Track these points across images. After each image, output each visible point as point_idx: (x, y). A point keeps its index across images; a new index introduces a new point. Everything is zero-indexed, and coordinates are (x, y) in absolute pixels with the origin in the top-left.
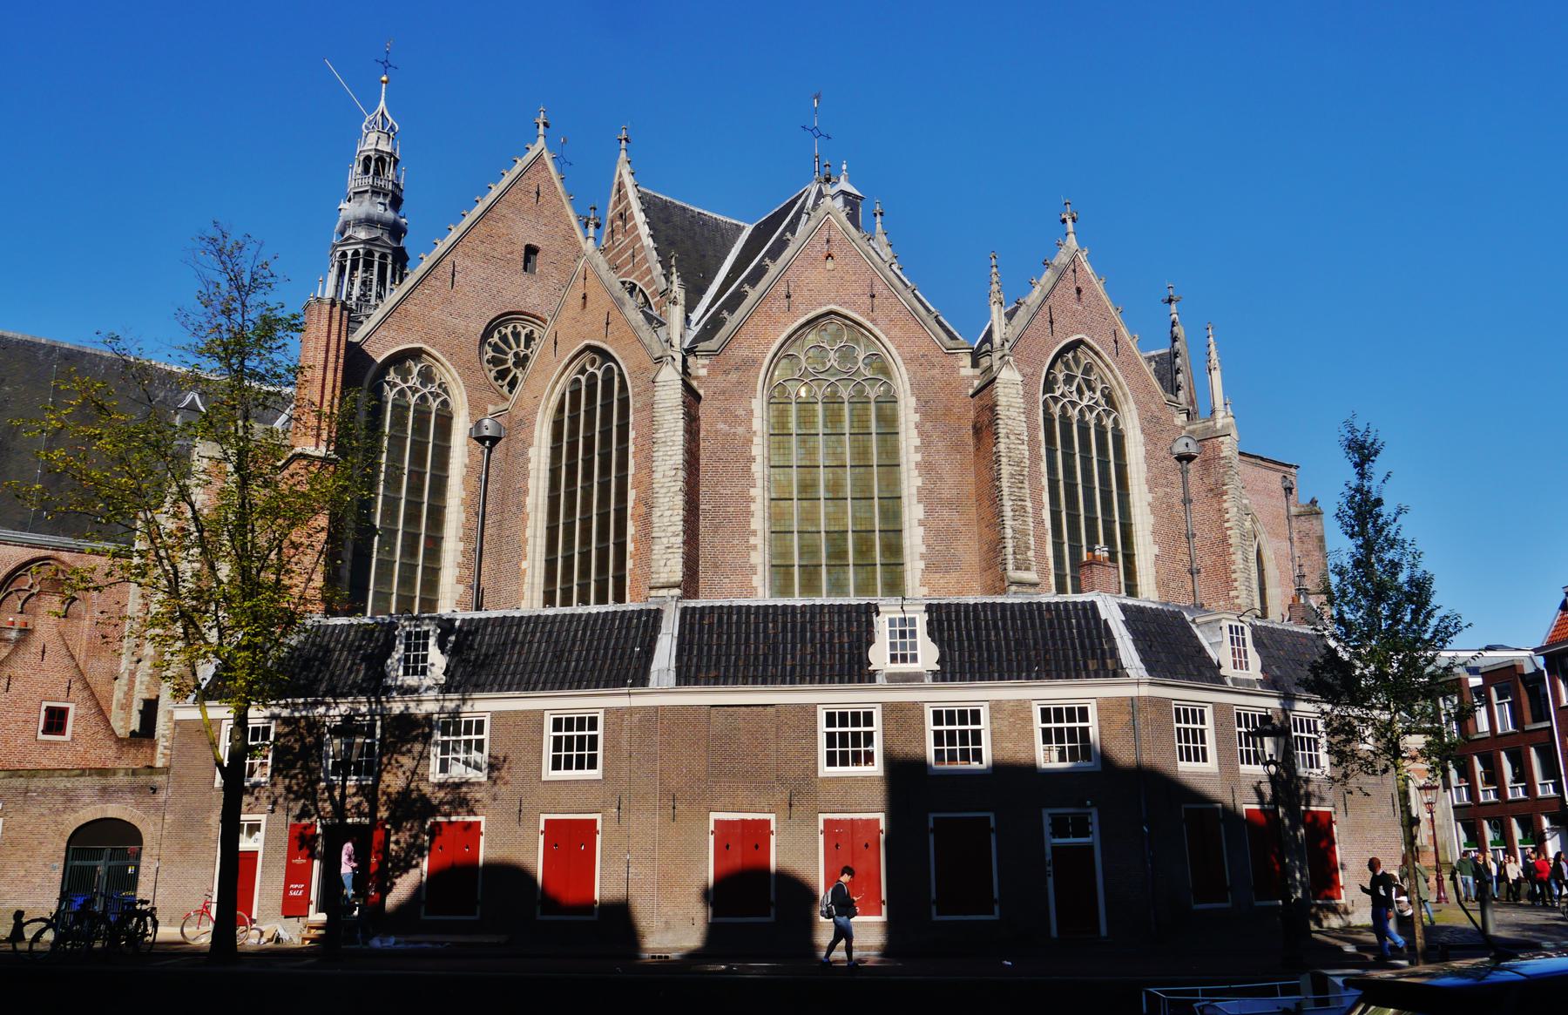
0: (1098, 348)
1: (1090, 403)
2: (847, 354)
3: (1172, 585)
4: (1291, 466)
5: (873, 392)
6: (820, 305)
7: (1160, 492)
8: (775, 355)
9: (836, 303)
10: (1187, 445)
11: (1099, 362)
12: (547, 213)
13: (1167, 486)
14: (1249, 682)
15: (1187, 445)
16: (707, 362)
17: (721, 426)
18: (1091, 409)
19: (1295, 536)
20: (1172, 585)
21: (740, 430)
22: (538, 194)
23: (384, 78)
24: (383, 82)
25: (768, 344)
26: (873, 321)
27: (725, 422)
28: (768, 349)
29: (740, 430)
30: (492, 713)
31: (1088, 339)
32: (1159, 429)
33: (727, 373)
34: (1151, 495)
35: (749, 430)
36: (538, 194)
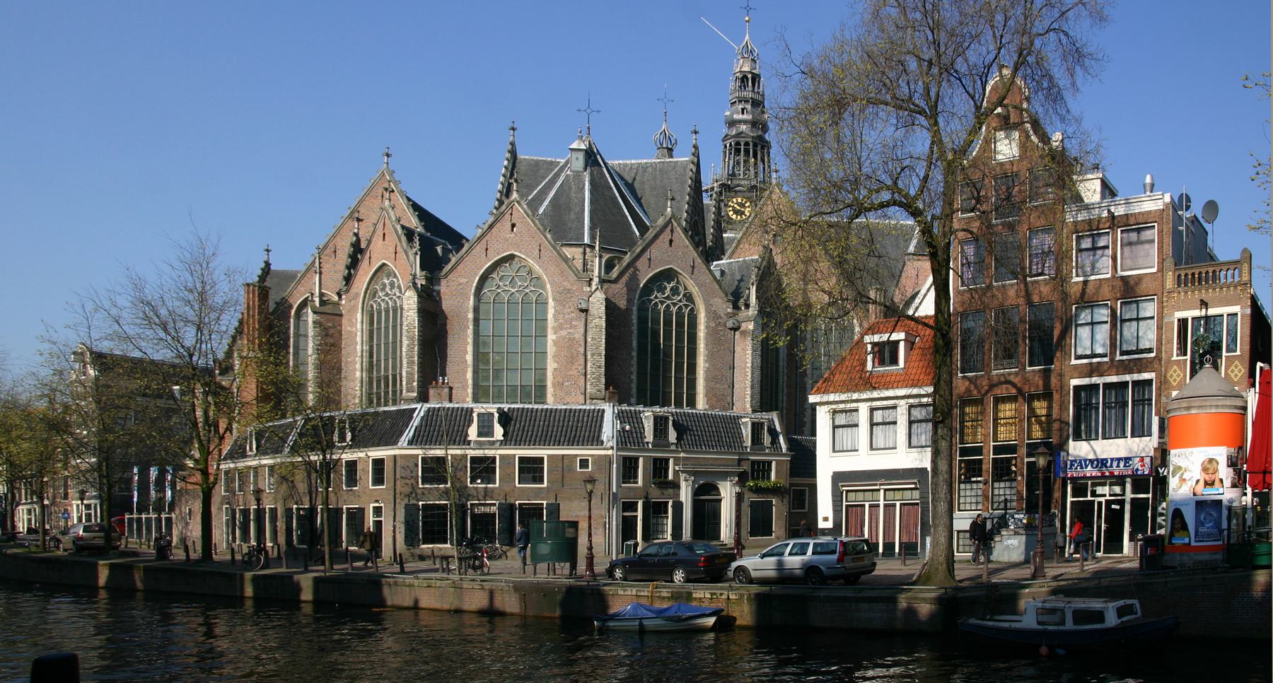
7: (564, 333)
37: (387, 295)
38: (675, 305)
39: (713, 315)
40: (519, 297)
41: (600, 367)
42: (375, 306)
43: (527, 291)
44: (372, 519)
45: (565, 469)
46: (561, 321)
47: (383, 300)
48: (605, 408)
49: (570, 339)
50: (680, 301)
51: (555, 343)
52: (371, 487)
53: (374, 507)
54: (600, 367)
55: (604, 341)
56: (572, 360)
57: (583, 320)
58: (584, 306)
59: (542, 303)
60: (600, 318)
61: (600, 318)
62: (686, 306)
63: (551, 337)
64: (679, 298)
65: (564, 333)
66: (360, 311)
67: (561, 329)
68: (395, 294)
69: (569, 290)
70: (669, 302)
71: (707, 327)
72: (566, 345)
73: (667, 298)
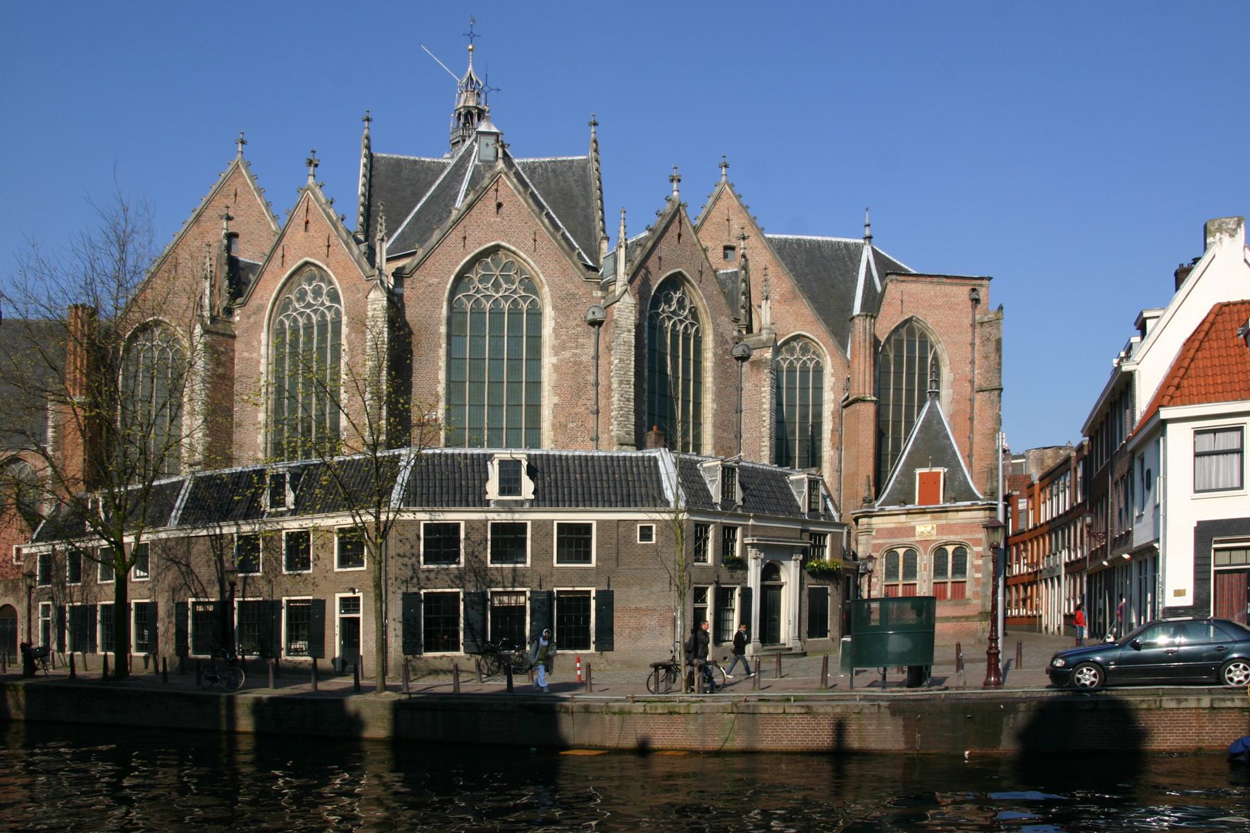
0: (513, 248)
1: (506, 294)
2: (317, 293)
3: (570, 425)
4: (982, 279)
5: (329, 316)
6: (300, 258)
7: (567, 354)
8: (276, 299)
9: (308, 256)
10: (594, 313)
11: (519, 259)
12: (243, 207)
13: (577, 348)
14: (522, 503)
15: (594, 313)
16: (239, 311)
17: (246, 354)
18: (506, 298)
19: (977, 341)
20: (570, 425)
21: (255, 355)
22: (236, 195)
23: (470, 47)
24: (470, 50)
25: (271, 293)
26: (328, 265)
27: (247, 351)
28: (270, 296)
29: (255, 355)
30: (597, 520)
31: (504, 244)
32: (574, 302)
33: (249, 317)
34: (556, 358)
35: (259, 355)
36: (236, 195)
37: (309, 305)
38: (681, 322)
39: (720, 340)
40: (506, 306)
41: (628, 400)
42: (287, 323)
43: (516, 296)
44: (338, 616)
45: (621, 542)
46: (563, 337)
47: (301, 314)
48: (657, 454)
49: (575, 363)
50: (686, 318)
51: (556, 368)
52: (336, 569)
53: (342, 599)
54: (628, 400)
55: (633, 363)
56: (578, 391)
57: (593, 337)
58: (599, 316)
59: (536, 316)
60: (629, 331)
61: (629, 331)
62: (692, 325)
63: (548, 360)
64: (685, 314)
65: (567, 354)
66: (265, 329)
67: (564, 349)
68: (323, 304)
69: (573, 295)
70: (676, 318)
71: (715, 354)
72: (570, 371)
73: (674, 312)
